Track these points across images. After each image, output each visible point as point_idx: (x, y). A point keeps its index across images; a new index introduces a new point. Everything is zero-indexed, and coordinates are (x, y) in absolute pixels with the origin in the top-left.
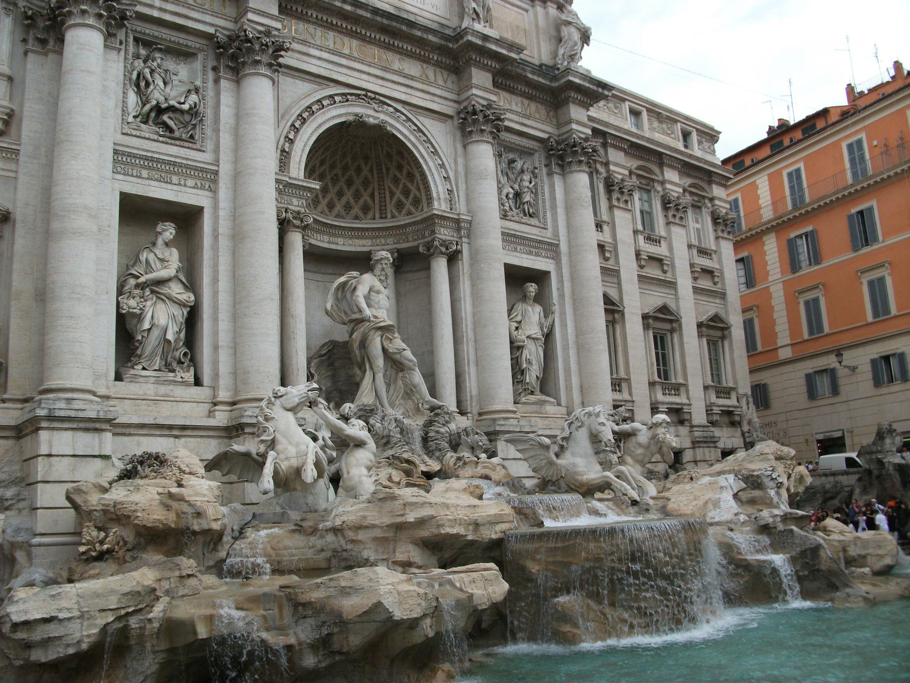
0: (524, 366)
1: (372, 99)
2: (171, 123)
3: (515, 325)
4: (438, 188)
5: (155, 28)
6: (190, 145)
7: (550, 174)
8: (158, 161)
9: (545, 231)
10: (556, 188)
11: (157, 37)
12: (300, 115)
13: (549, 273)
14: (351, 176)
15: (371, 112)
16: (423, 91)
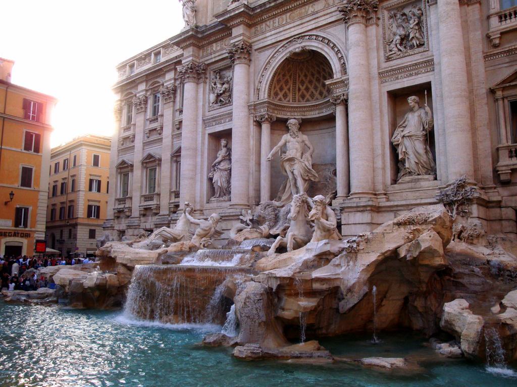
0: (400, 157)
1: (298, 38)
2: (222, 99)
3: (402, 129)
4: (335, 65)
5: (217, 64)
6: (228, 105)
7: (429, 6)
8: (216, 117)
9: (426, 53)
10: (431, 16)
11: (218, 68)
12: (265, 68)
13: (430, 82)
14: (323, 75)
15: (298, 45)
16: (324, 15)
